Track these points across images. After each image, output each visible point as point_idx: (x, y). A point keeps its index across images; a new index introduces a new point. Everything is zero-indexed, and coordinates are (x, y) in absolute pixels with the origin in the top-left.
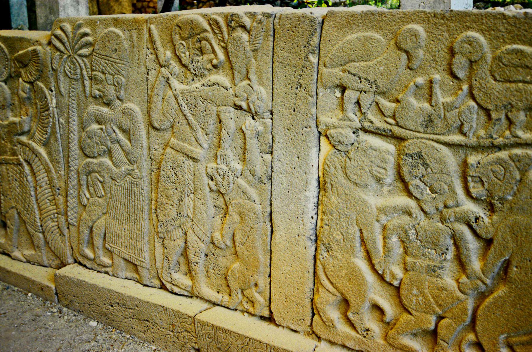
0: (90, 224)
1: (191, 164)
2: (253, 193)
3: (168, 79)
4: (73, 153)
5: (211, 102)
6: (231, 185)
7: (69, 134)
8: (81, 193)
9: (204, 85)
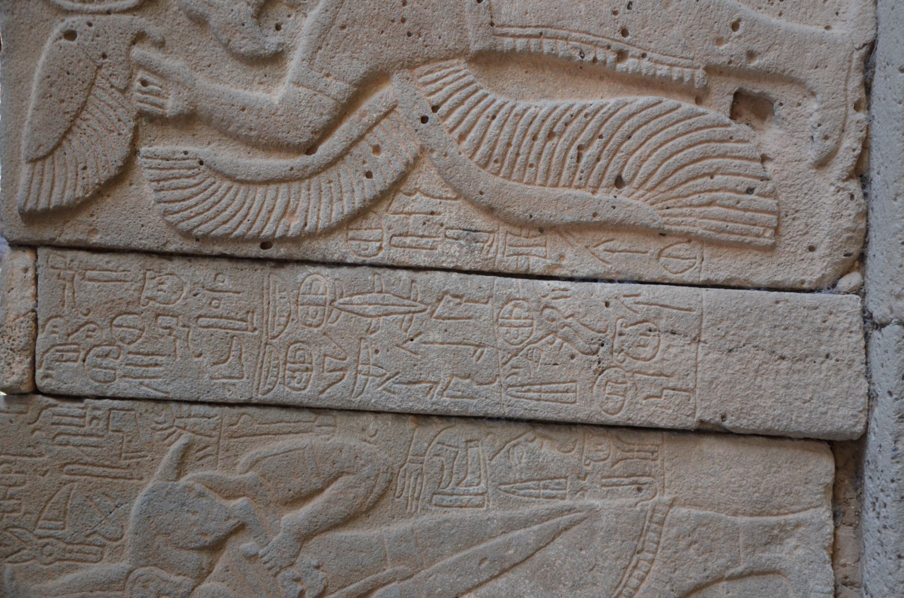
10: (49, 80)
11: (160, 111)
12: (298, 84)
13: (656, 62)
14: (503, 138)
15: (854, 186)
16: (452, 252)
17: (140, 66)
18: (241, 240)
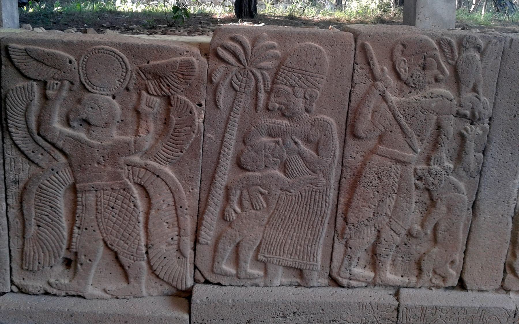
0: (238, 239)
1: (399, 167)
2: (462, 185)
4: (222, 168)
5: (432, 112)
6: (443, 182)
7: (221, 148)
8: (228, 208)
9: (425, 97)
10: (53, 55)
11: (48, 88)
12: (60, 132)
13: (77, 238)
14: (48, 193)
15: (42, 291)
16: (11, 177)
17: (62, 83)
18: (6, 114)
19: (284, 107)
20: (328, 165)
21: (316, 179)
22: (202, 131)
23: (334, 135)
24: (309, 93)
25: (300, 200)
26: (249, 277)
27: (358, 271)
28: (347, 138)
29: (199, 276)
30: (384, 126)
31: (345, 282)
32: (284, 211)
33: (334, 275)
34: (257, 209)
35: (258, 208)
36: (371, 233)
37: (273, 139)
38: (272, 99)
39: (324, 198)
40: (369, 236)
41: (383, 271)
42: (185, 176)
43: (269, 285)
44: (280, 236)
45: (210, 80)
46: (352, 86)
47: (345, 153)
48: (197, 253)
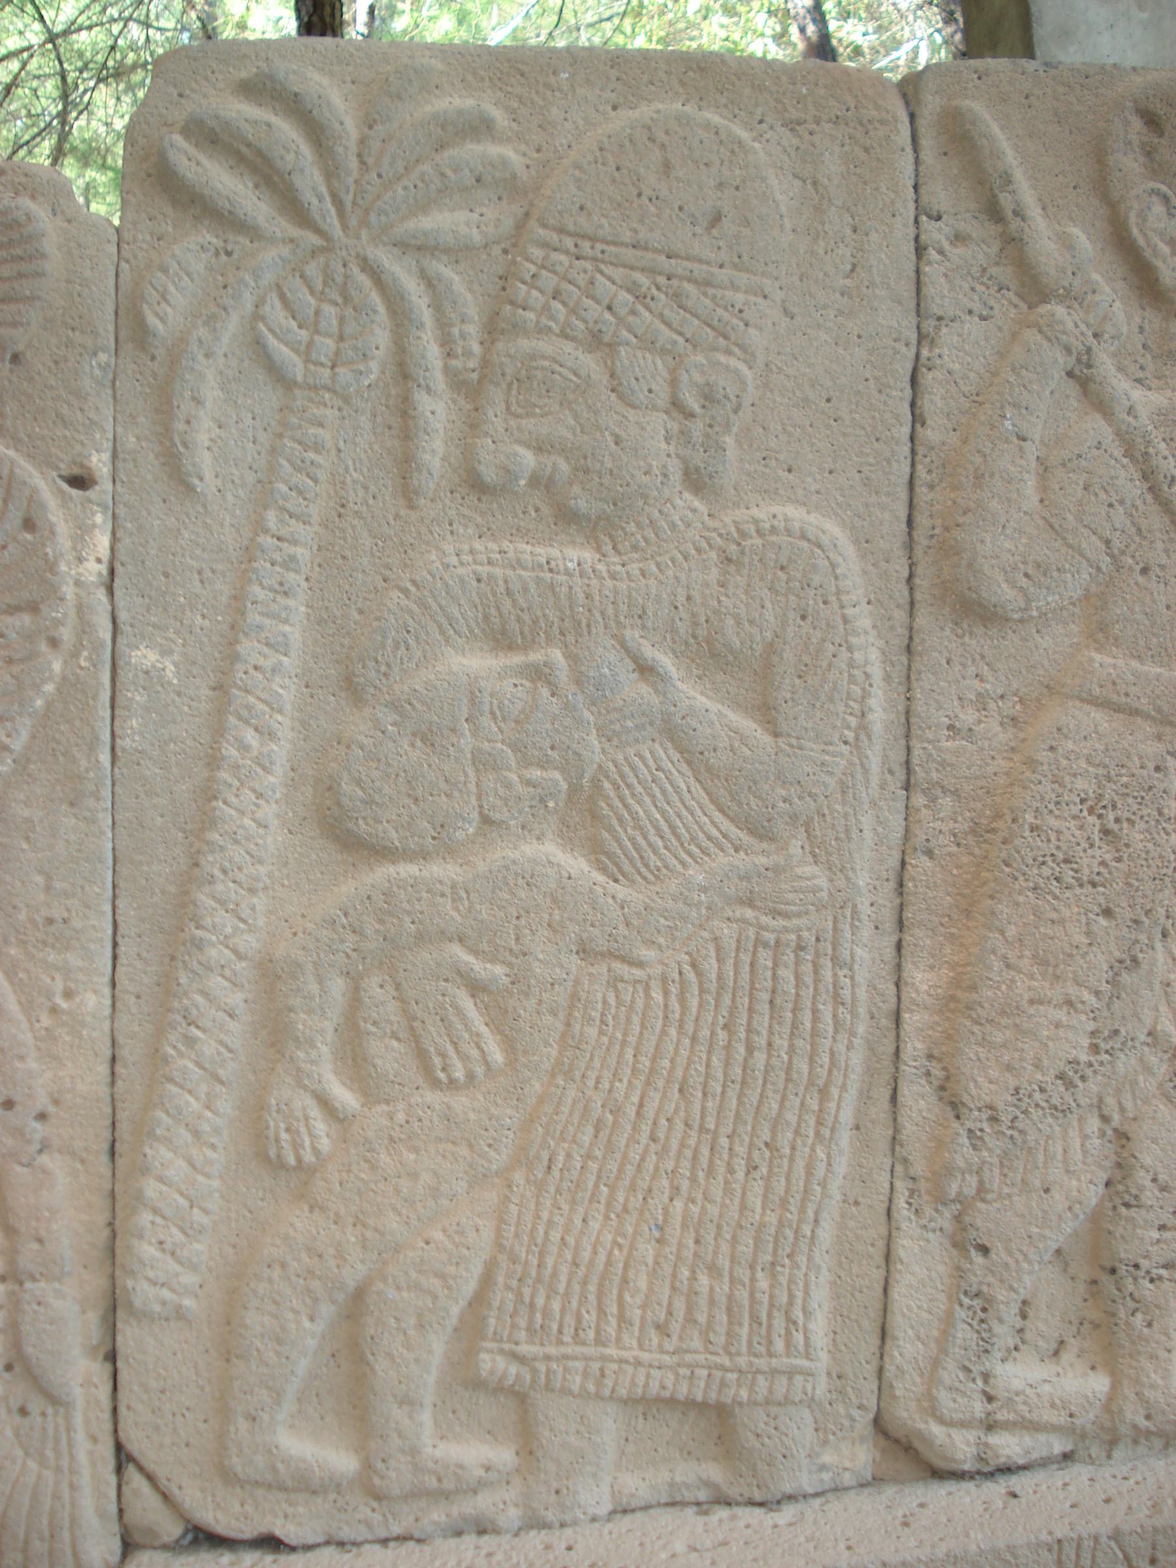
0: (354, 1273)
3: (1086, 359)
4: (237, 853)
7: (219, 732)
19: (564, 466)
20: (831, 782)
21: (777, 870)
22: (107, 636)
23: (850, 612)
24: (698, 378)
25: (694, 1003)
26: (432, 1483)
27: (1020, 1375)
28: (921, 621)
29: (146, 1506)
30: (1108, 542)
31: (961, 1446)
32: (607, 1075)
33: (905, 1413)
34: (452, 1081)
35: (459, 1074)
36: (1085, 1152)
37: (517, 659)
38: (495, 419)
39: (827, 974)
40: (1074, 1174)
41: (1153, 1357)
42: (22, 917)
43: (550, 1516)
44: (595, 1225)
45: (133, 330)
46: (921, 337)
47: (919, 707)
48: (123, 1376)
